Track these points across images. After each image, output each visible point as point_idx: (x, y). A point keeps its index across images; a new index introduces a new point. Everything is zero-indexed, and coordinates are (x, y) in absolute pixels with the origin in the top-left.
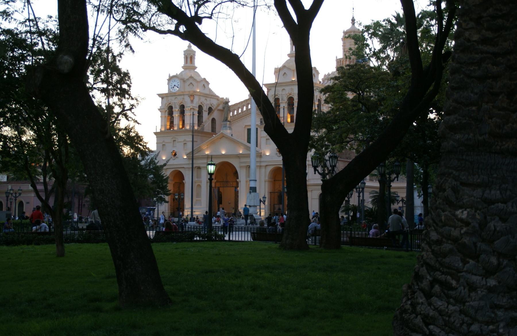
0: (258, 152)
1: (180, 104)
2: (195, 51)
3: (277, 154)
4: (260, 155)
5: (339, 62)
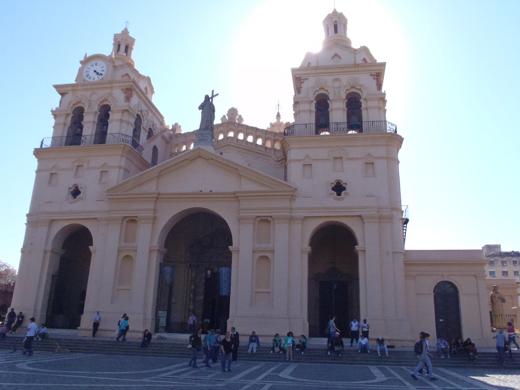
0: (291, 187)
1: (101, 102)
2: (135, 40)
3: (331, 194)
4: (292, 193)
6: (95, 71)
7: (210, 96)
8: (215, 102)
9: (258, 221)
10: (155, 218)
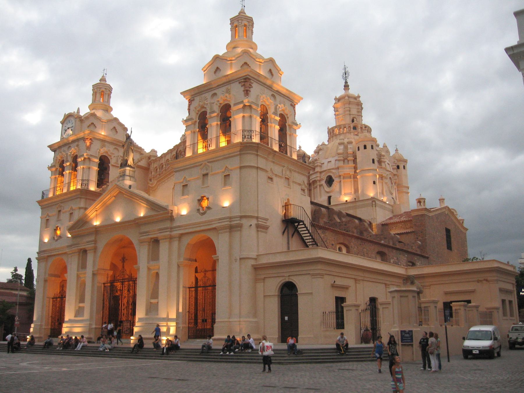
5: (332, 132)
9: (153, 242)
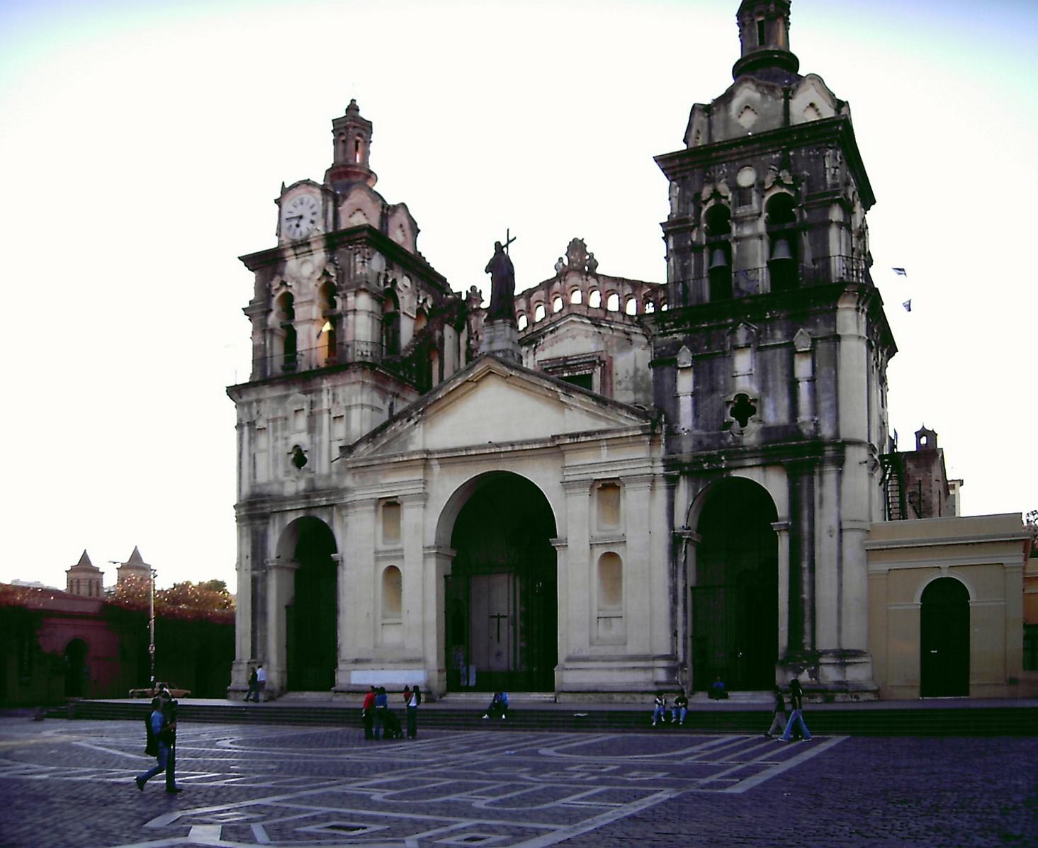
6: (301, 217)
7: (503, 243)
8: (513, 253)
9: (598, 489)
10: (425, 497)
